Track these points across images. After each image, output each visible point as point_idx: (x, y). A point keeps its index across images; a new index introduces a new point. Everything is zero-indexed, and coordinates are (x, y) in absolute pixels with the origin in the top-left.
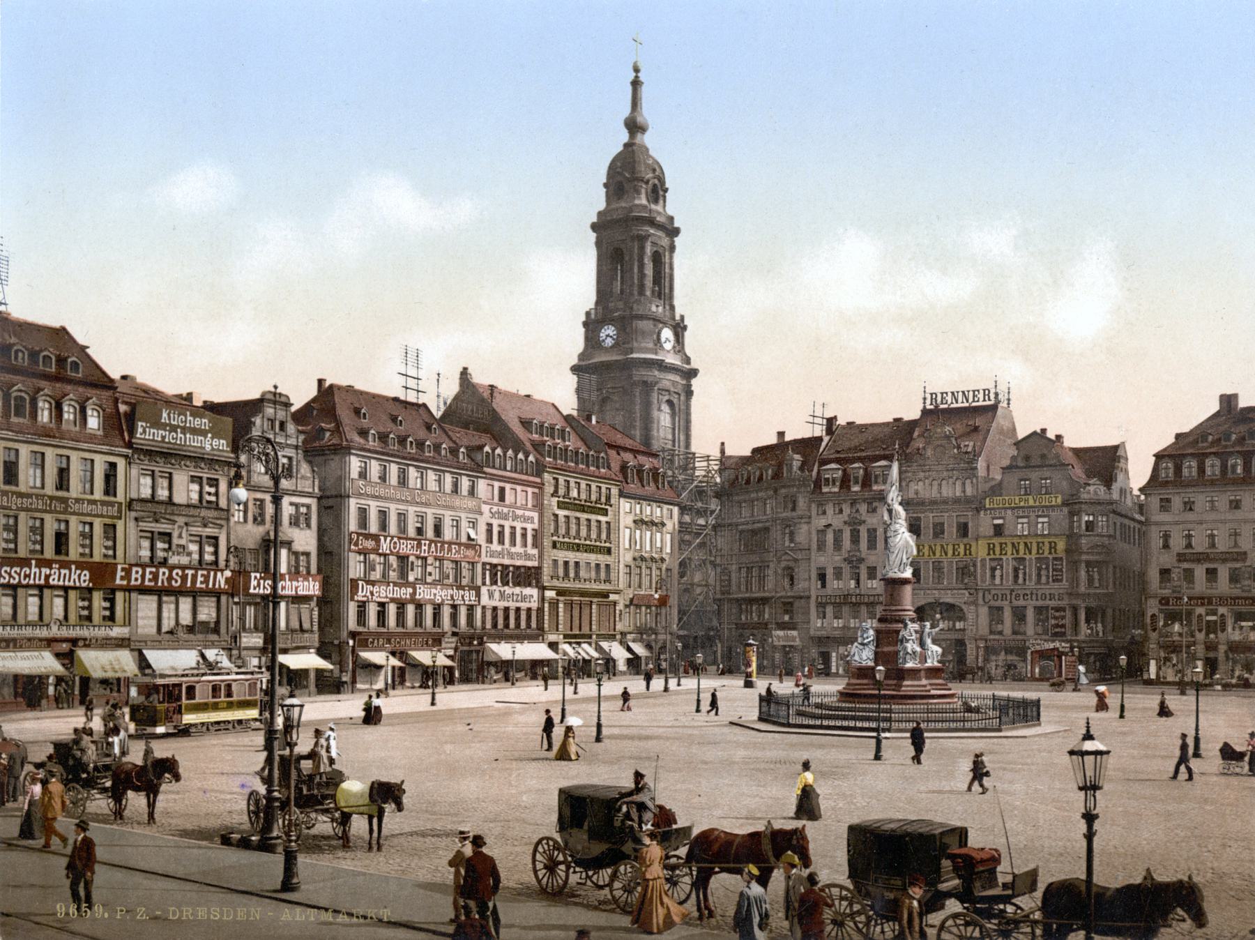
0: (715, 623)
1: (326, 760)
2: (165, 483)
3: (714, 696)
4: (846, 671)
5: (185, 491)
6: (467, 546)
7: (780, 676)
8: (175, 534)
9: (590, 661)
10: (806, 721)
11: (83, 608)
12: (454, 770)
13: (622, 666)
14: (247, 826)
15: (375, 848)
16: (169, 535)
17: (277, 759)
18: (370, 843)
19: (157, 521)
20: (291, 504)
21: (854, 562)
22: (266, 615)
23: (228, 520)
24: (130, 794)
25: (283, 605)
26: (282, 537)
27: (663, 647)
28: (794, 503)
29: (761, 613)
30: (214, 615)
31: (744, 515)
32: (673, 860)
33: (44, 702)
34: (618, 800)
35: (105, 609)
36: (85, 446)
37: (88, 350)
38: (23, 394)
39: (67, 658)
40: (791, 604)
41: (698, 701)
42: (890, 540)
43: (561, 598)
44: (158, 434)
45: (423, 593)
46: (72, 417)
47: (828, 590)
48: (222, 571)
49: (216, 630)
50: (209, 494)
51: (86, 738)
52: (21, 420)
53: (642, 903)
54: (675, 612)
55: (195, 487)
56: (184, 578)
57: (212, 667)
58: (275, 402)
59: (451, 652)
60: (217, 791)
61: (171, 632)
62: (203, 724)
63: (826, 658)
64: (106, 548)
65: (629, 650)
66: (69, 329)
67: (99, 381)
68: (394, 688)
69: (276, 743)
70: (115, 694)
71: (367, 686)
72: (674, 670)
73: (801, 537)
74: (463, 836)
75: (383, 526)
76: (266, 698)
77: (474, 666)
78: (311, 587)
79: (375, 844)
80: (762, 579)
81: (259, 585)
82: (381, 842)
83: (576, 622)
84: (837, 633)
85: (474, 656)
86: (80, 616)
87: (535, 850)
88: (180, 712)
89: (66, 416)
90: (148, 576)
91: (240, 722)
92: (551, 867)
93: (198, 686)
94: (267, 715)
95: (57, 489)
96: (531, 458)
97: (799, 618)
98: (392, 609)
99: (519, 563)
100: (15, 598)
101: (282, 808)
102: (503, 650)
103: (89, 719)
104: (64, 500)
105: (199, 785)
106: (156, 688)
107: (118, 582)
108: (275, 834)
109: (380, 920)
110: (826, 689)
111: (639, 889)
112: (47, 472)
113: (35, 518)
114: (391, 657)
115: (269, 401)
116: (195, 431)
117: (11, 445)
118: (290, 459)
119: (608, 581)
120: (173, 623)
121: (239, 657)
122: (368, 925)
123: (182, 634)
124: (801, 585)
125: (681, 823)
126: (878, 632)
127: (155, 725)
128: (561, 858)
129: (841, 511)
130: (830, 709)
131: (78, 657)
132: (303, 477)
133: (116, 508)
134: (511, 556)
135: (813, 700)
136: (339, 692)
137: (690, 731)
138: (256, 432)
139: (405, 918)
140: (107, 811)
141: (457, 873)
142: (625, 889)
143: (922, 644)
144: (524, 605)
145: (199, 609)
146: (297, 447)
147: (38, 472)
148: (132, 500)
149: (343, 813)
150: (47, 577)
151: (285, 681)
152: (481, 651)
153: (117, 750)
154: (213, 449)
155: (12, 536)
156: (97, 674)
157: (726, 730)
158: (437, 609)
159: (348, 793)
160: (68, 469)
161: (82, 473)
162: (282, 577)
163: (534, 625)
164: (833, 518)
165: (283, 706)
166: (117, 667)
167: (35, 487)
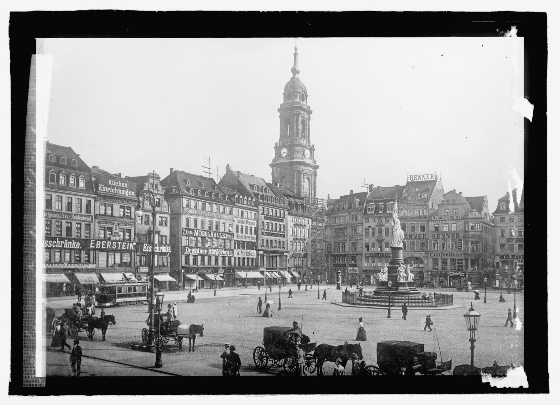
1: (173, 316)
2: (110, 208)
3: (325, 292)
4: (377, 283)
5: (118, 211)
6: (228, 234)
7: (351, 285)
8: (114, 229)
10: (361, 302)
11: (77, 257)
13: (289, 281)
15: (192, 350)
16: (111, 228)
18: (190, 349)
19: (106, 223)
20: (160, 217)
21: (380, 241)
22: (149, 260)
23: (135, 223)
24: (95, 329)
25: (156, 256)
27: (305, 273)
30: (129, 260)
37: (79, 156)
38: (54, 173)
40: (355, 257)
41: (319, 294)
43: (265, 254)
45: (211, 252)
46: (73, 182)
47: (370, 252)
48: (132, 243)
49: (130, 266)
50: (127, 213)
51: (79, 308)
52: (53, 183)
55: (122, 210)
56: (117, 245)
58: (153, 177)
59: (222, 275)
61: (112, 266)
62: (124, 302)
63: (369, 277)
64: (87, 233)
65: (292, 274)
68: (199, 289)
69: (153, 310)
71: (189, 288)
73: (359, 230)
75: (196, 225)
78: (167, 249)
79: (192, 349)
81: (147, 248)
82: (194, 348)
85: (231, 276)
89: (71, 182)
90: (103, 245)
91: (139, 301)
93: (122, 288)
95: (67, 210)
96: (254, 200)
98: (199, 258)
100: (50, 253)
102: (242, 274)
103: (80, 300)
104: (70, 215)
107: (91, 247)
110: (369, 290)
113: (58, 222)
114: (198, 277)
115: (151, 177)
116: (122, 188)
118: (159, 199)
120: (113, 263)
121: (139, 276)
123: (116, 267)
126: (389, 268)
127: (106, 303)
129: (375, 221)
133: (90, 218)
134: (246, 238)
138: (146, 189)
140: (86, 336)
143: (406, 273)
145: (123, 257)
146: (162, 195)
147: (60, 204)
148: (97, 215)
149: (179, 337)
150: (63, 245)
151: (157, 285)
153: (90, 312)
156: (83, 282)
160: (71, 203)
161: (77, 204)
163: (254, 264)
165: (156, 295)
166: (90, 280)
167: (58, 210)
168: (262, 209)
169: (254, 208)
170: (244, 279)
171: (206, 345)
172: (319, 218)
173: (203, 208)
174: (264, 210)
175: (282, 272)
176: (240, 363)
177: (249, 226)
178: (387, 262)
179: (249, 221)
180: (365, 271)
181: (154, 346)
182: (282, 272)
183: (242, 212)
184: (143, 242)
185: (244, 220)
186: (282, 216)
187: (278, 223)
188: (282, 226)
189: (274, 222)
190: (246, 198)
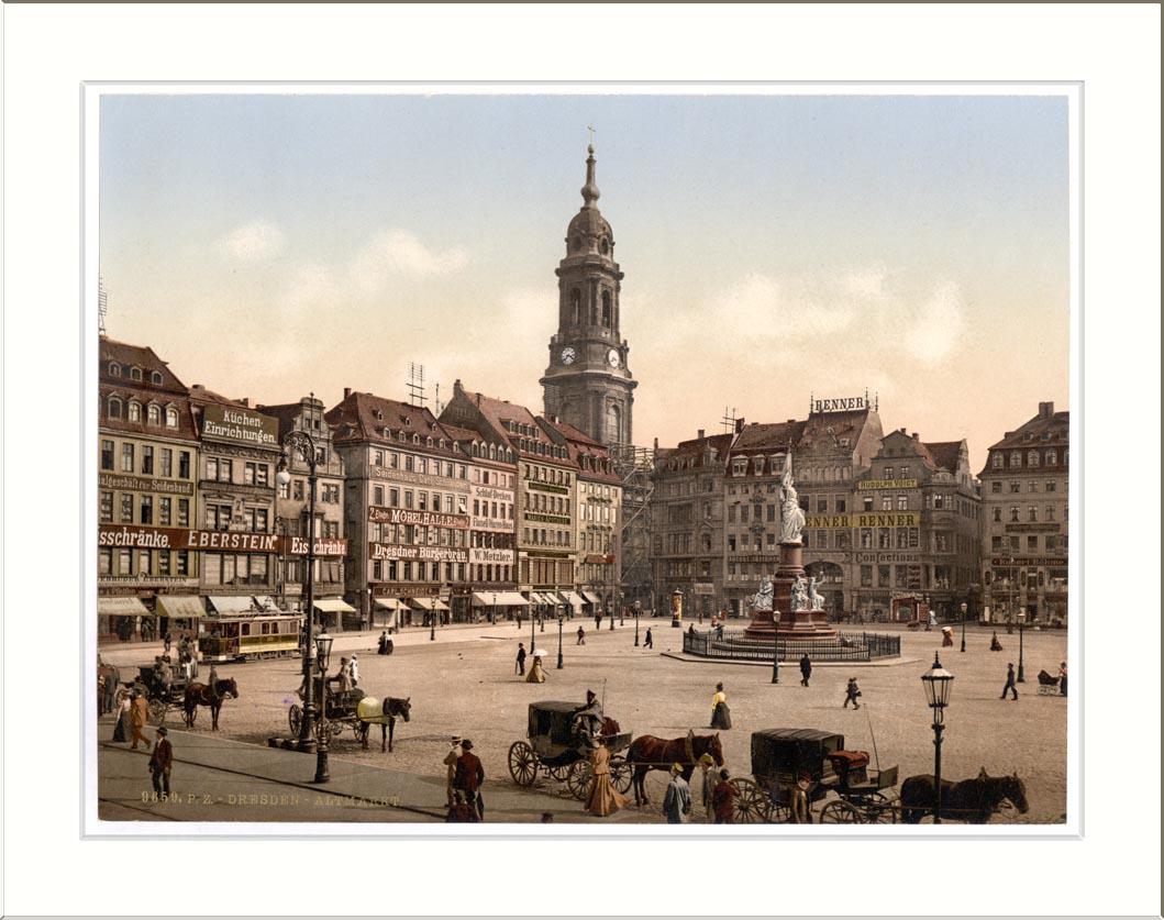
0: (650, 577)
1: (349, 682)
2: (227, 468)
3: (649, 633)
4: (750, 614)
5: (242, 474)
6: (459, 518)
7: (700, 618)
8: (234, 508)
9: (553, 606)
10: (720, 653)
11: (163, 564)
12: (448, 689)
13: (578, 610)
14: (289, 732)
15: (388, 750)
16: (230, 508)
17: (312, 680)
18: (383, 746)
19: (220, 497)
20: (324, 484)
21: (757, 531)
22: (304, 570)
23: (275, 496)
24: (199, 706)
25: (317, 562)
26: (316, 510)
27: (610, 596)
28: (711, 485)
29: (685, 571)
30: (264, 569)
31: (672, 494)
32: (617, 760)
33: (133, 636)
34: (574, 713)
35: (180, 565)
36: (165, 439)
39: (151, 602)
40: (709, 563)
41: (637, 638)
42: (785, 514)
44: (221, 430)
45: (425, 553)
46: (155, 417)
47: (738, 553)
48: (270, 536)
49: (265, 582)
50: (261, 476)
51: (165, 664)
52: (116, 419)
53: (593, 792)
54: (619, 568)
55: (250, 471)
56: (241, 541)
57: (262, 610)
59: (446, 599)
60: (266, 705)
61: (230, 583)
62: (255, 653)
63: (735, 604)
64: (181, 518)
65: (584, 598)
66: (153, 349)
67: (177, 389)
68: (402, 627)
69: (311, 669)
70: (187, 630)
71: (382, 625)
72: (619, 614)
73: (716, 512)
74: (455, 741)
75: (395, 502)
76: (304, 634)
77: (464, 610)
78: (339, 549)
79: (387, 746)
80: (686, 543)
81: (298, 547)
82: (392, 744)
83: (543, 576)
84: (743, 586)
85: (465, 602)
86: (161, 571)
87: (511, 752)
88: (237, 645)
89: (150, 416)
90: (213, 540)
91: (284, 652)
92: (523, 765)
93: (251, 625)
94: (305, 647)
97: (714, 574)
98: (401, 566)
99: (499, 531)
100: (111, 556)
101: (316, 719)
102: (486, 598)
103: (168, 650)
104: (149, 481)
105: (252, 700)
106: (219, 626)
107: (190, 544)
108: (310, 738)
109: (391, 805)
110: (735, 628)
111: (591, 782)
112: (136, 459)
113: (126, 495)
114: (400, 603)
115: (307, 405)
116: (250, 428)
117: (108, 438)
118: (323, 450)
119: (567, 544)
120: (232, 576)
121: (283, 602)
122: (382, 809)
123: (239, 585)
124: (716, 549)
125: (623, 731)
126: (775, 584)
127: (218, 655)
128: (530, 758)
129: (747, 492)
130: (738, 643)
131: (161, 606)
132: (333, 464)
134: (493, 525)
135: (725, 637)
136: (360, 630)
137: (629, 661)
138: (297, 429)
139: (410, 804)
140: (181, 720)
141: (450, 769)
142: (579, 782)
143: (809, 594)
144: (502, 563)
145: (253, 565)
146: (328, 441)
147: (129, 459)
149: (362, 722)
150: (136, 540)
151: (318, 620)
152: (470, 597)
153: (189, 674)
154: (263, 442)
155: (108, 508)
156: (174, 615)
157: (658, 660)
158: (436, 565)
159: (367, 708)
160: (152, 457)
162: (317, 541)
163: (510, 578)
164: (740, 496)
165: (317, 640)
166: (189, 610)
167: (126, 471)
168: (525, 468)
169: (509, 466)
170: (490, 608)
171: (415, 739)
172: (638, 486)
173: (410, 467)
174: (528, 472)
175: (565, 594)
176: (481, 774)
177: (499, 501)
178: (771, 572)
179: (499, 491)
180: (731, 591)
181: (312, 741)
182: (565, 594)
183: (486, 474)
184: (291, 534)
185: (489, 490)
186: (564, 482)
187: (556, 495)
188: (565, 502)
189: (549, 495)
190: (492, 445)
